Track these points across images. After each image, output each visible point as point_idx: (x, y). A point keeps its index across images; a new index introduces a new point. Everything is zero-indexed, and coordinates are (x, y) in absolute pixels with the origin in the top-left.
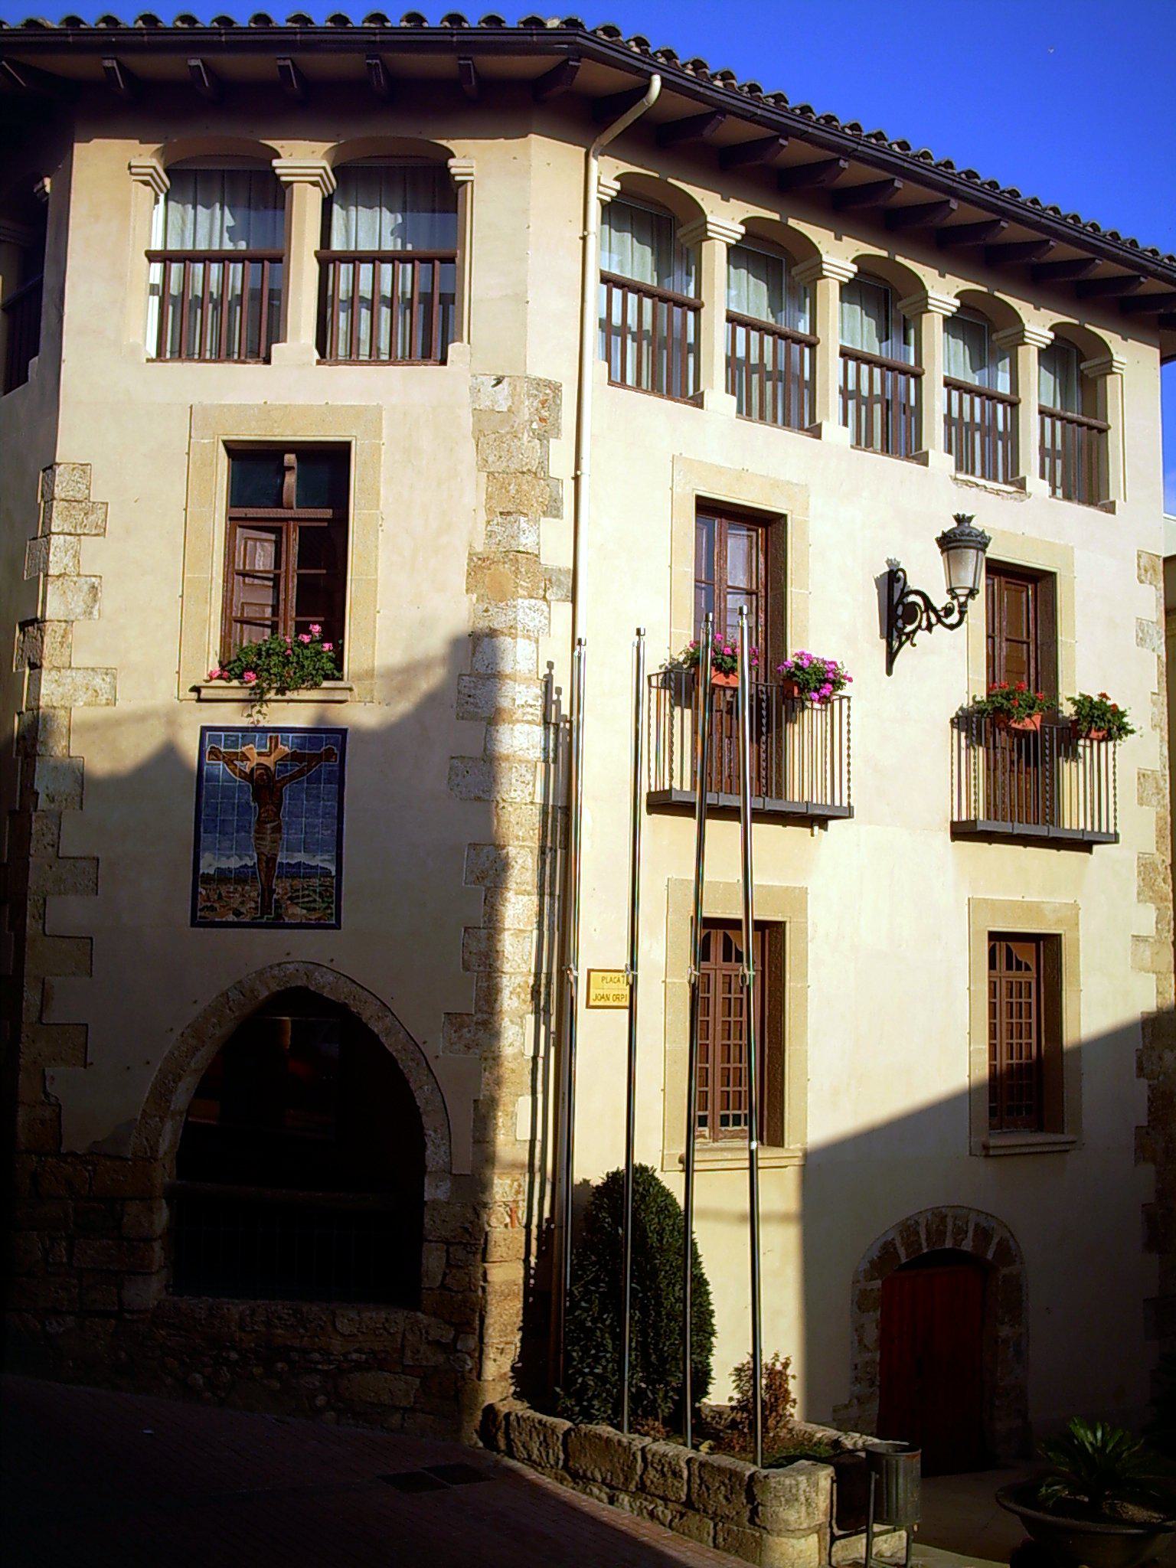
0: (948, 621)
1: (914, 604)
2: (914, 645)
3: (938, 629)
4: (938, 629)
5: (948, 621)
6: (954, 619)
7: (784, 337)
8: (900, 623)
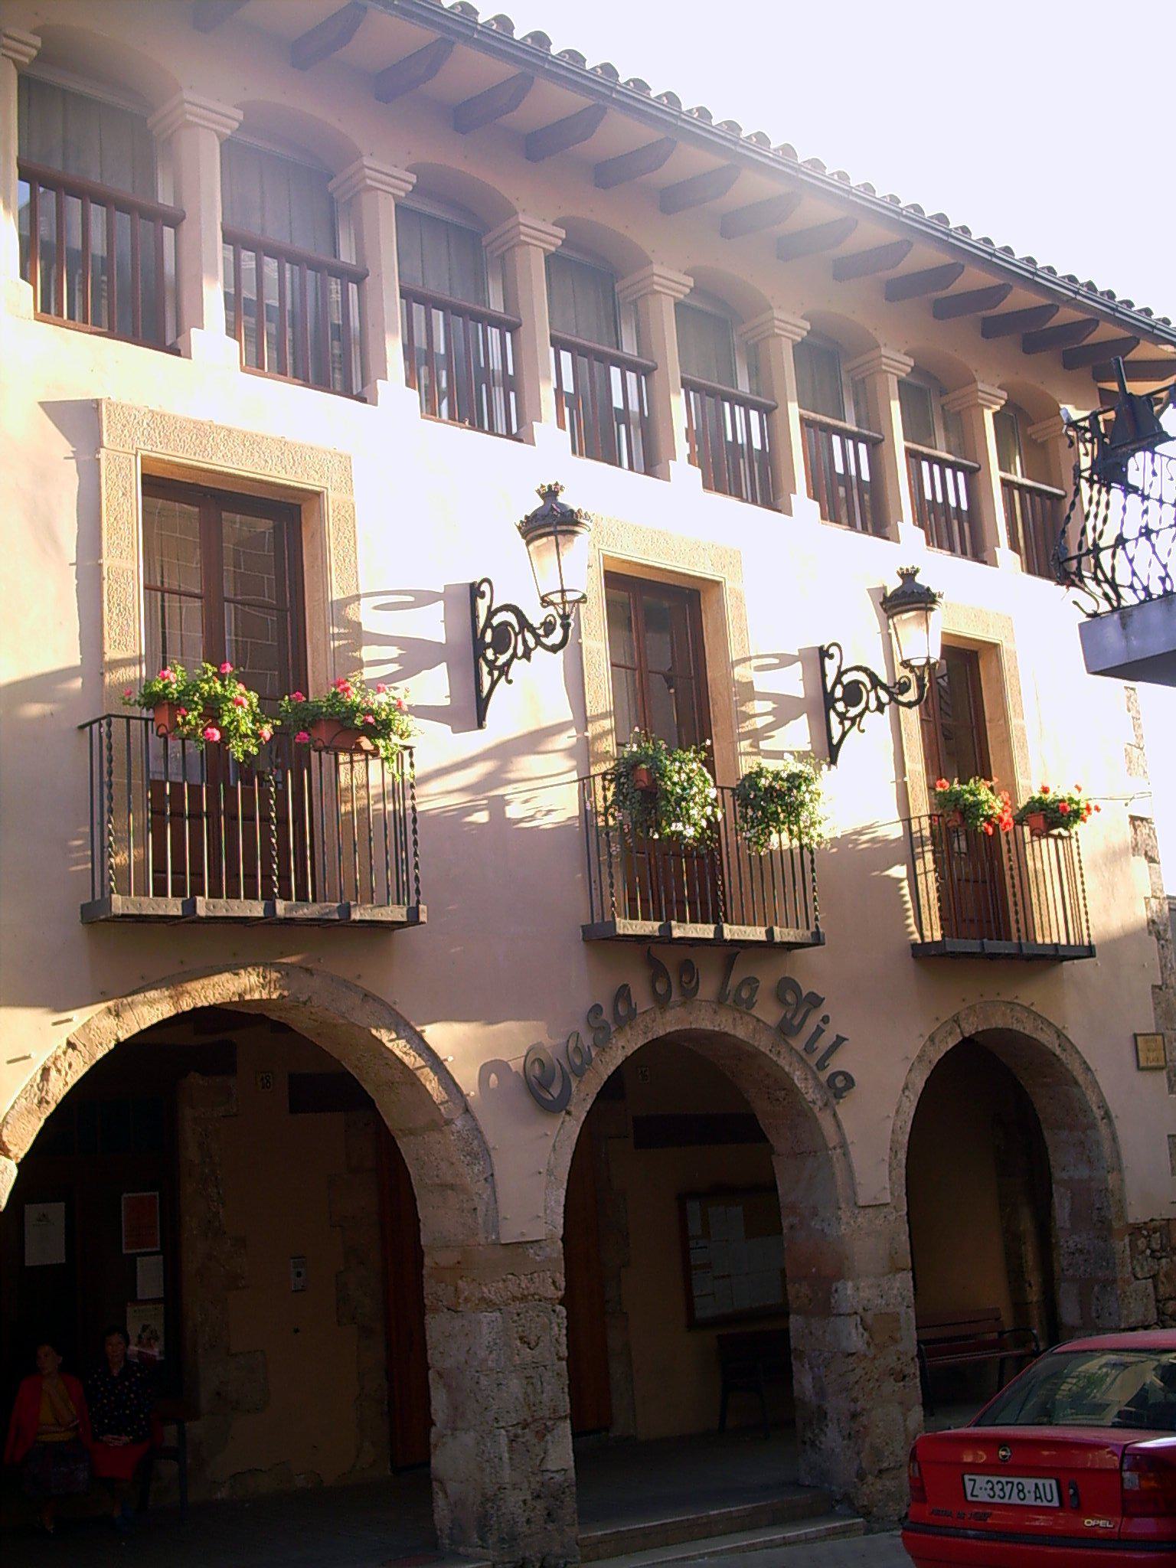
0: (903, 698)
1: (856, 683)
2: (510, 682)
3: (538, 653)
4: (538, 653)
5: (903, 698)
6: (556, 637)
7: (316, 266)
8: (490, 654)
